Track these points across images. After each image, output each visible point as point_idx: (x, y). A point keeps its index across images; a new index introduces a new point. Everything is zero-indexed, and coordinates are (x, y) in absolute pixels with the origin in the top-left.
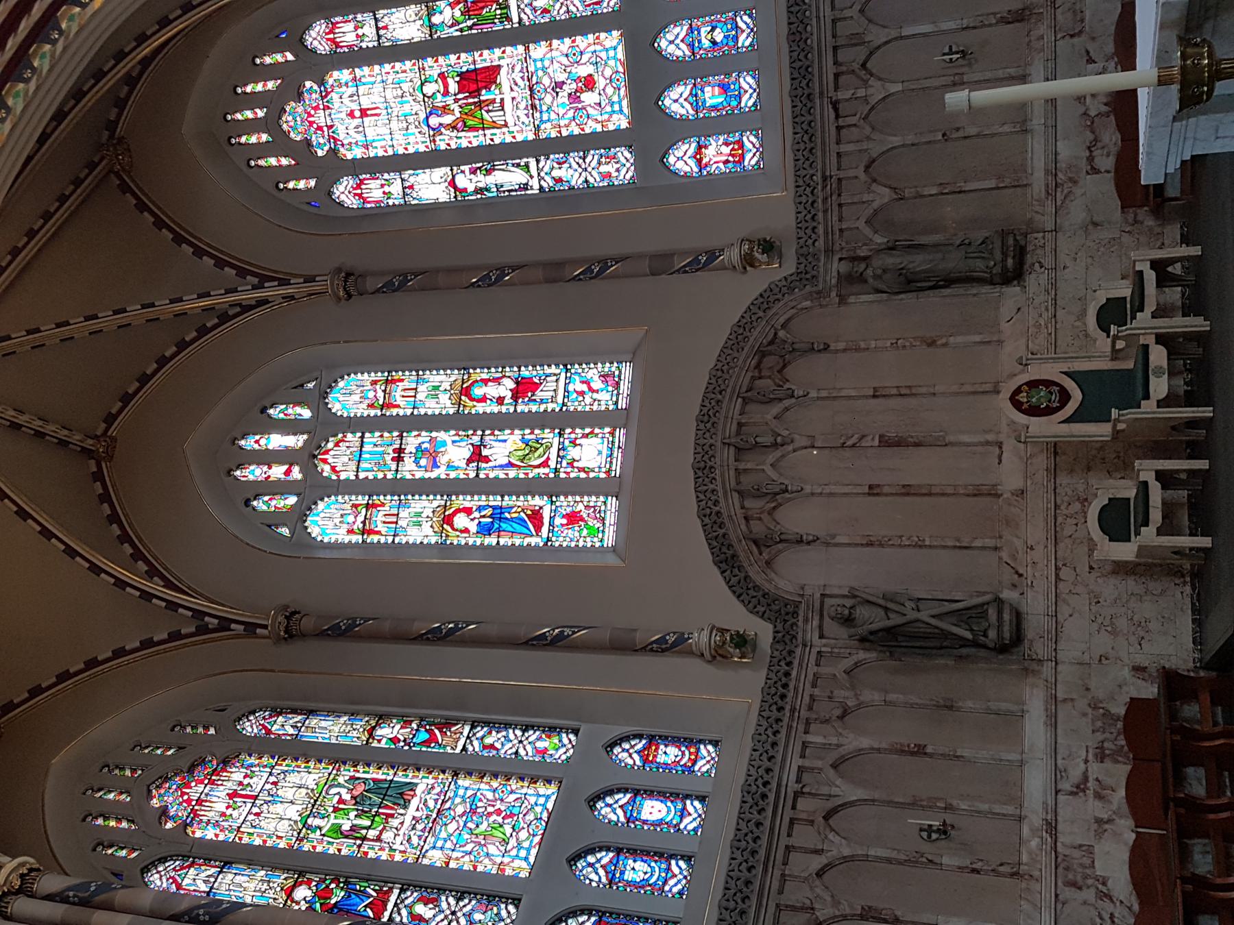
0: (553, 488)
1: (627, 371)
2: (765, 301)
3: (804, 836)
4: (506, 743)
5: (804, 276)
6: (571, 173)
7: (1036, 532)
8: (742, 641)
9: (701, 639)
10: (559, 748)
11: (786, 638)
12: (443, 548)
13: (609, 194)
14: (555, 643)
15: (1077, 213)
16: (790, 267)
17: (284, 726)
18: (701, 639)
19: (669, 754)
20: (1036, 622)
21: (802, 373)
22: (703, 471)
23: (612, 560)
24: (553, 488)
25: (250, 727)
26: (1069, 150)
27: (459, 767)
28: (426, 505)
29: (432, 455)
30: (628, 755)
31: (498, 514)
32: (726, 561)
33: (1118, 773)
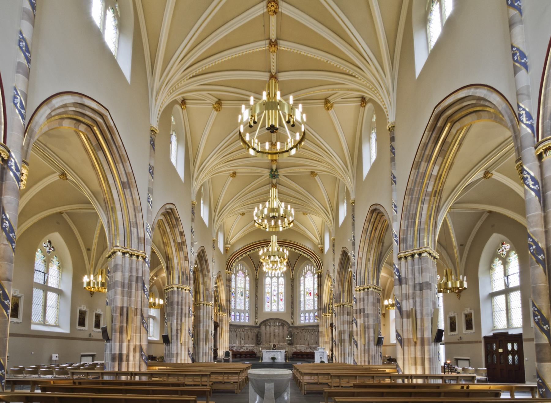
0: (271, 304)
1: (283, 310)
2: (288, 324)
3: (241, 330)
4: (247, 304)
5: (290, 327)
6: (302, 304)
7: (267, 345)
8: (257, 323)
9: (257, 320)
10: (247, 309)
11: (257, 327)
12: (265, 293)
13: (300, 308)
14: (256, 307)
15: (294, 349)
16: (291, 325)
17: (247, 282)
18: (257, 320)
19: (247, 318)
20: (259, 346)
21: (281, 327)
22: (272, 319)
23: (264, 311)
24: (271, 304)
25: (247, 278)
26: (298, 348)
27: (245, 300)
28: (270, 291)
29: (275, 291)
30: (247, 315)
31: (268, 298)
32: (264, 322)
33: (248, 350)
